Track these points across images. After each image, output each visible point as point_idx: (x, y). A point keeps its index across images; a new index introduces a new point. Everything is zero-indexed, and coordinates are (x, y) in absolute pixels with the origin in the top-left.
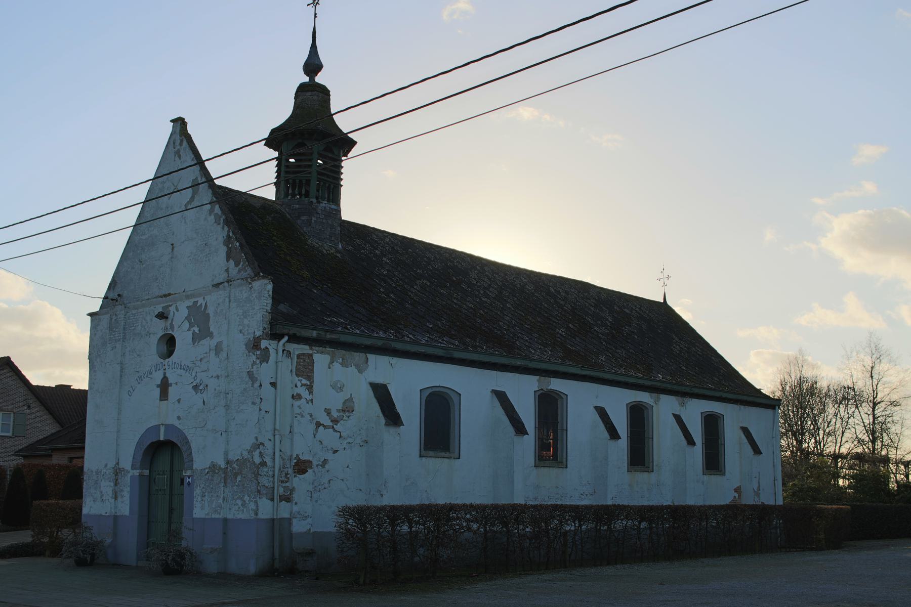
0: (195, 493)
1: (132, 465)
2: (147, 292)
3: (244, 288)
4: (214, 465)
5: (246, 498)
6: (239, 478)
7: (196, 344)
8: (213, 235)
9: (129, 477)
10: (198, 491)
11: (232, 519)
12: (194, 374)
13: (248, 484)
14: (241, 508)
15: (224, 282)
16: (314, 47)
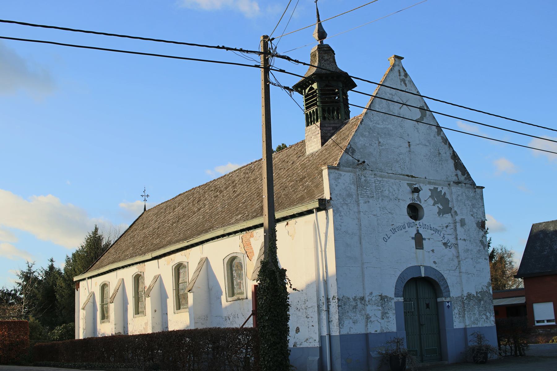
0: (453, 312)
1: (395, 293)
5: (488, 314)
6: (482, 302)
7: (441, 215)
9: (393, 303)
10: (456, 311)
11: (481, 327)
12: (442, 235)
13: (488, 306)
14: (486, 320)
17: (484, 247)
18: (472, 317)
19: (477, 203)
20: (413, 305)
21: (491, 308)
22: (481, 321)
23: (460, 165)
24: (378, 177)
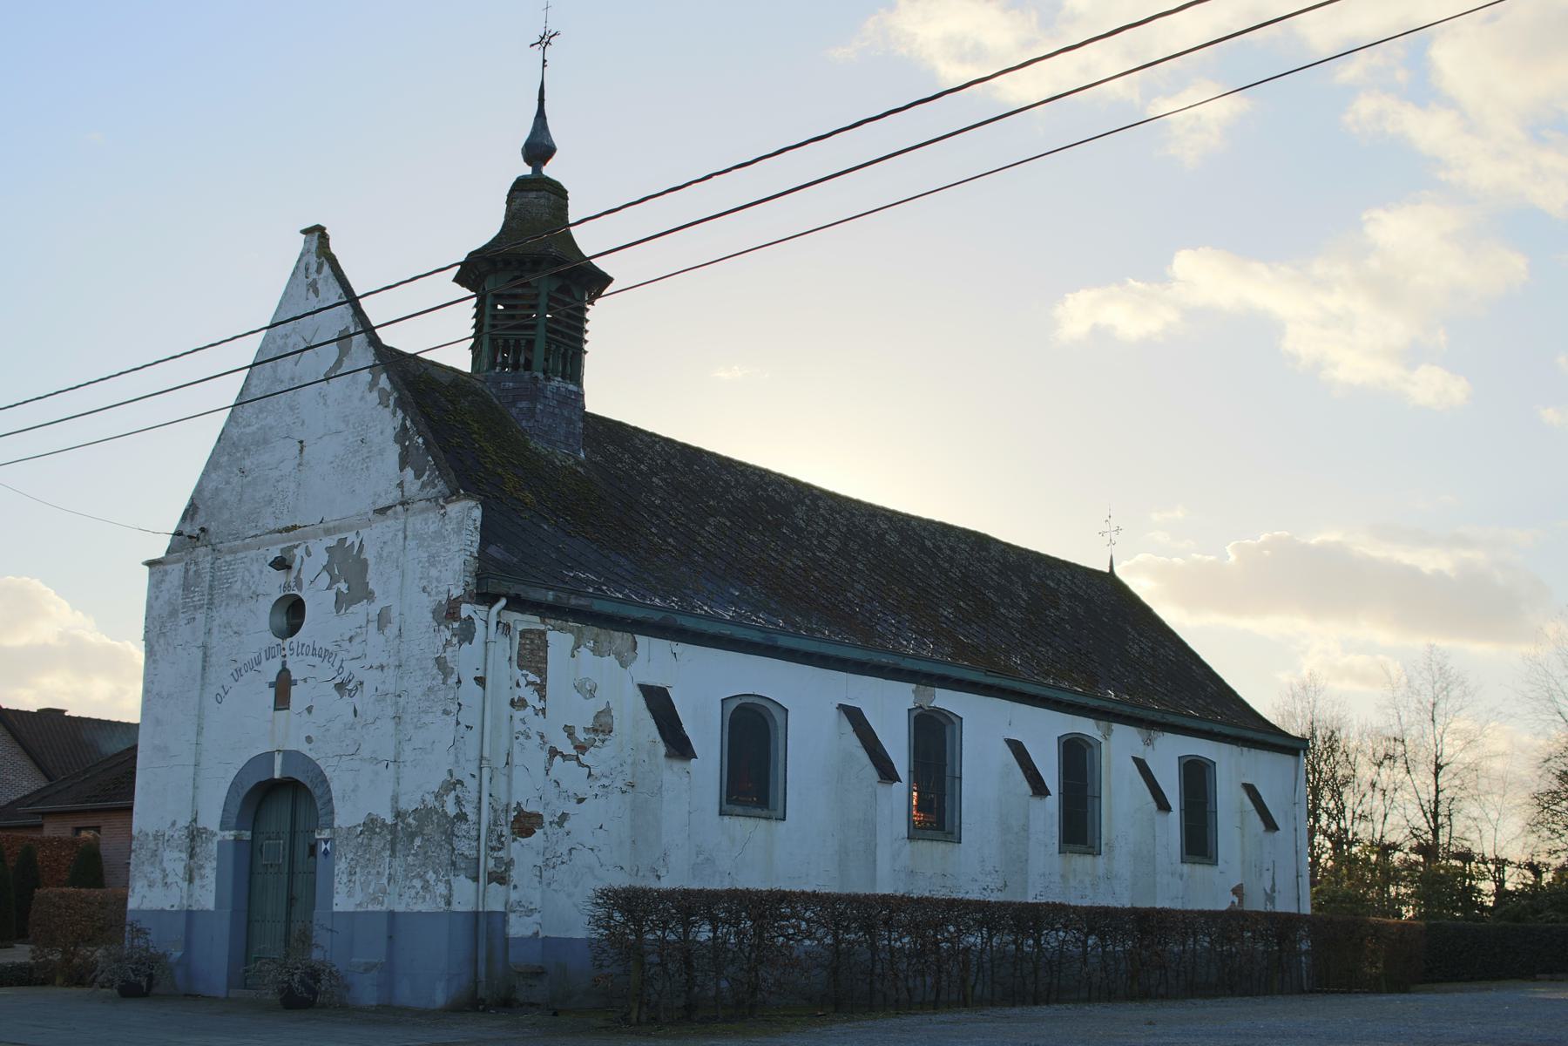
0: (336, 868)
1: (221, 822)
2: (254, 525)
3: (432, 515)
4: (372, 819)
5: (431, 876)
6: (418, 842)
8: (375, 426)
9: (215, 844)
10: (341, 866)
12: (337, 664)
15: (395, 506)
16: (541, 115)
17: (445, 677)
18: (373, 884)
19: (443, 550)
20: (281, 848)
21: (442, 858)
22: (407, 895)
23: (415, 452)
24: (226, 554)
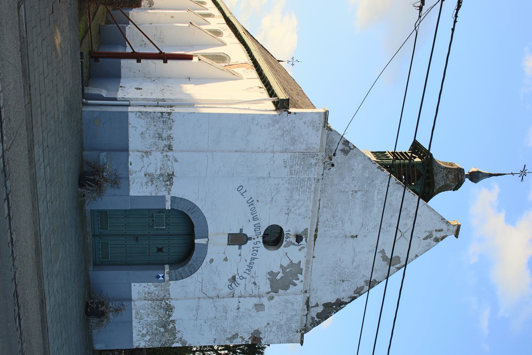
0: (151, 284)
2: (325, 205)
3: (299, 324)
4: (172, 309)
5: (148, 338)
6: (162, 330)
7: (269, 277)
8: (348, 286)
11: (132, 325)
12: (245, 275)
13: (158, 338)
14: (141, 333)
15: (307, 310)
16: (490, 175)
17: (230, 339)
19: (283, 333)
20: (161, 227)
21: (155, 342)
22: (140, 326)
